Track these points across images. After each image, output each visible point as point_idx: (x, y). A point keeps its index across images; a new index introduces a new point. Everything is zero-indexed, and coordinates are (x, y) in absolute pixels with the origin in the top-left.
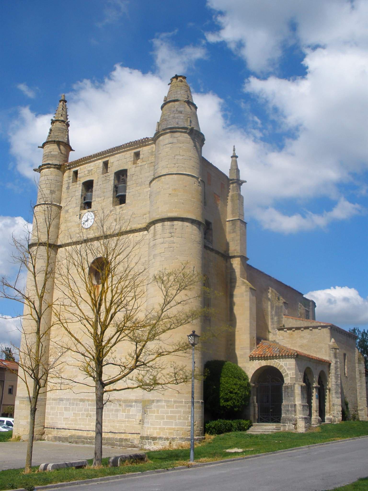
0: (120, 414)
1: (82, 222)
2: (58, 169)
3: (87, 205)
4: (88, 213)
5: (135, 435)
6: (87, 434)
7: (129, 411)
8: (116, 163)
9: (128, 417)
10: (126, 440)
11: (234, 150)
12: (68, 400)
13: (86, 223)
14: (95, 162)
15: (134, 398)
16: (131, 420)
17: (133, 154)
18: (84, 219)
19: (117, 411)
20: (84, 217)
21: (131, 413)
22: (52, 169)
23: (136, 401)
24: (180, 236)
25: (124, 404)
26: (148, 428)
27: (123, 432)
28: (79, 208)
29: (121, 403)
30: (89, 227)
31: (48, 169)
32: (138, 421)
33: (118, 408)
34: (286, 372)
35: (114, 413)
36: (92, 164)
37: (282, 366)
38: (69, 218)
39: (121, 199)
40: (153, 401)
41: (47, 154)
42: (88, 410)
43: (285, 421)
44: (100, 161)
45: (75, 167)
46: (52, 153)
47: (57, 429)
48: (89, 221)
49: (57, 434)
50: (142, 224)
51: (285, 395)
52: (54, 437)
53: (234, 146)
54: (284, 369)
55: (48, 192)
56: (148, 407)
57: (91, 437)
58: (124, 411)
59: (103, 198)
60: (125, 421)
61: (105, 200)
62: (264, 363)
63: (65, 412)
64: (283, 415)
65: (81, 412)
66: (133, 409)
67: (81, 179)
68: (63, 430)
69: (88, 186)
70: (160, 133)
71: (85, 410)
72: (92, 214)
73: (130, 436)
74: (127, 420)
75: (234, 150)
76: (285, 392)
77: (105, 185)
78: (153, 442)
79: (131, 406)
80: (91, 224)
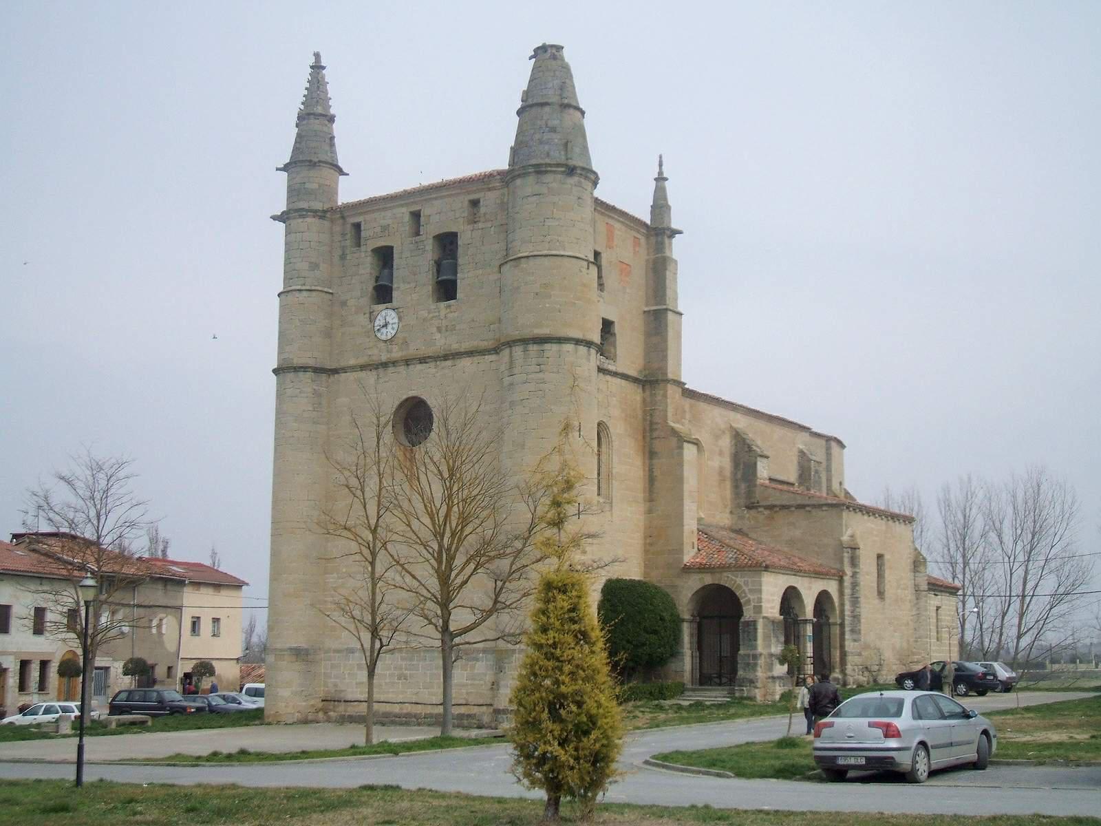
1: (376, 328)
2: (321, 218)
3: (383, 294)
5: (485, 708)
6: (401, 709)
7: (473, 667)
10: (469, 716)
11: (661, 165)
13: (384, 330)
14: (395, 211)
16: (477, 682)
17: (466, 203)
18: (379, 322)
20: (379, 317)
21: (476, 671)
22: (309, 220)
24: (555, 370)
27: (464, 702)
30: (389, 337)
31: (300, 220)
34: (746, 596)
36: (389, 214)
37: (739, 586)
39: (446, 290)
42: (401, 669)
43: (743, 682)
44: (404, 210)
45: (355, 215)
46: (307, 185)
48: (390, 327)
49: (345, 711)
50: (487, 340)
51: (744, 638)
53: (661, 157)
54: (744, 592)
55: (305, 266)
56: (506, 661)
57: (407, 714)
59: (413, 285)
60: (467, 685)
61: (417, 289)
62: (708, 579)
63: (359, 672)
64: (741, 673)
66: (479, 664)
67: (369, 242)
69: (385, 256)
70: (517, 173)
72: (393, 314)
73: (475, 710)
74: (469, 682)
75: (661, 165)
76: (744, 632)
79: (477, 660)
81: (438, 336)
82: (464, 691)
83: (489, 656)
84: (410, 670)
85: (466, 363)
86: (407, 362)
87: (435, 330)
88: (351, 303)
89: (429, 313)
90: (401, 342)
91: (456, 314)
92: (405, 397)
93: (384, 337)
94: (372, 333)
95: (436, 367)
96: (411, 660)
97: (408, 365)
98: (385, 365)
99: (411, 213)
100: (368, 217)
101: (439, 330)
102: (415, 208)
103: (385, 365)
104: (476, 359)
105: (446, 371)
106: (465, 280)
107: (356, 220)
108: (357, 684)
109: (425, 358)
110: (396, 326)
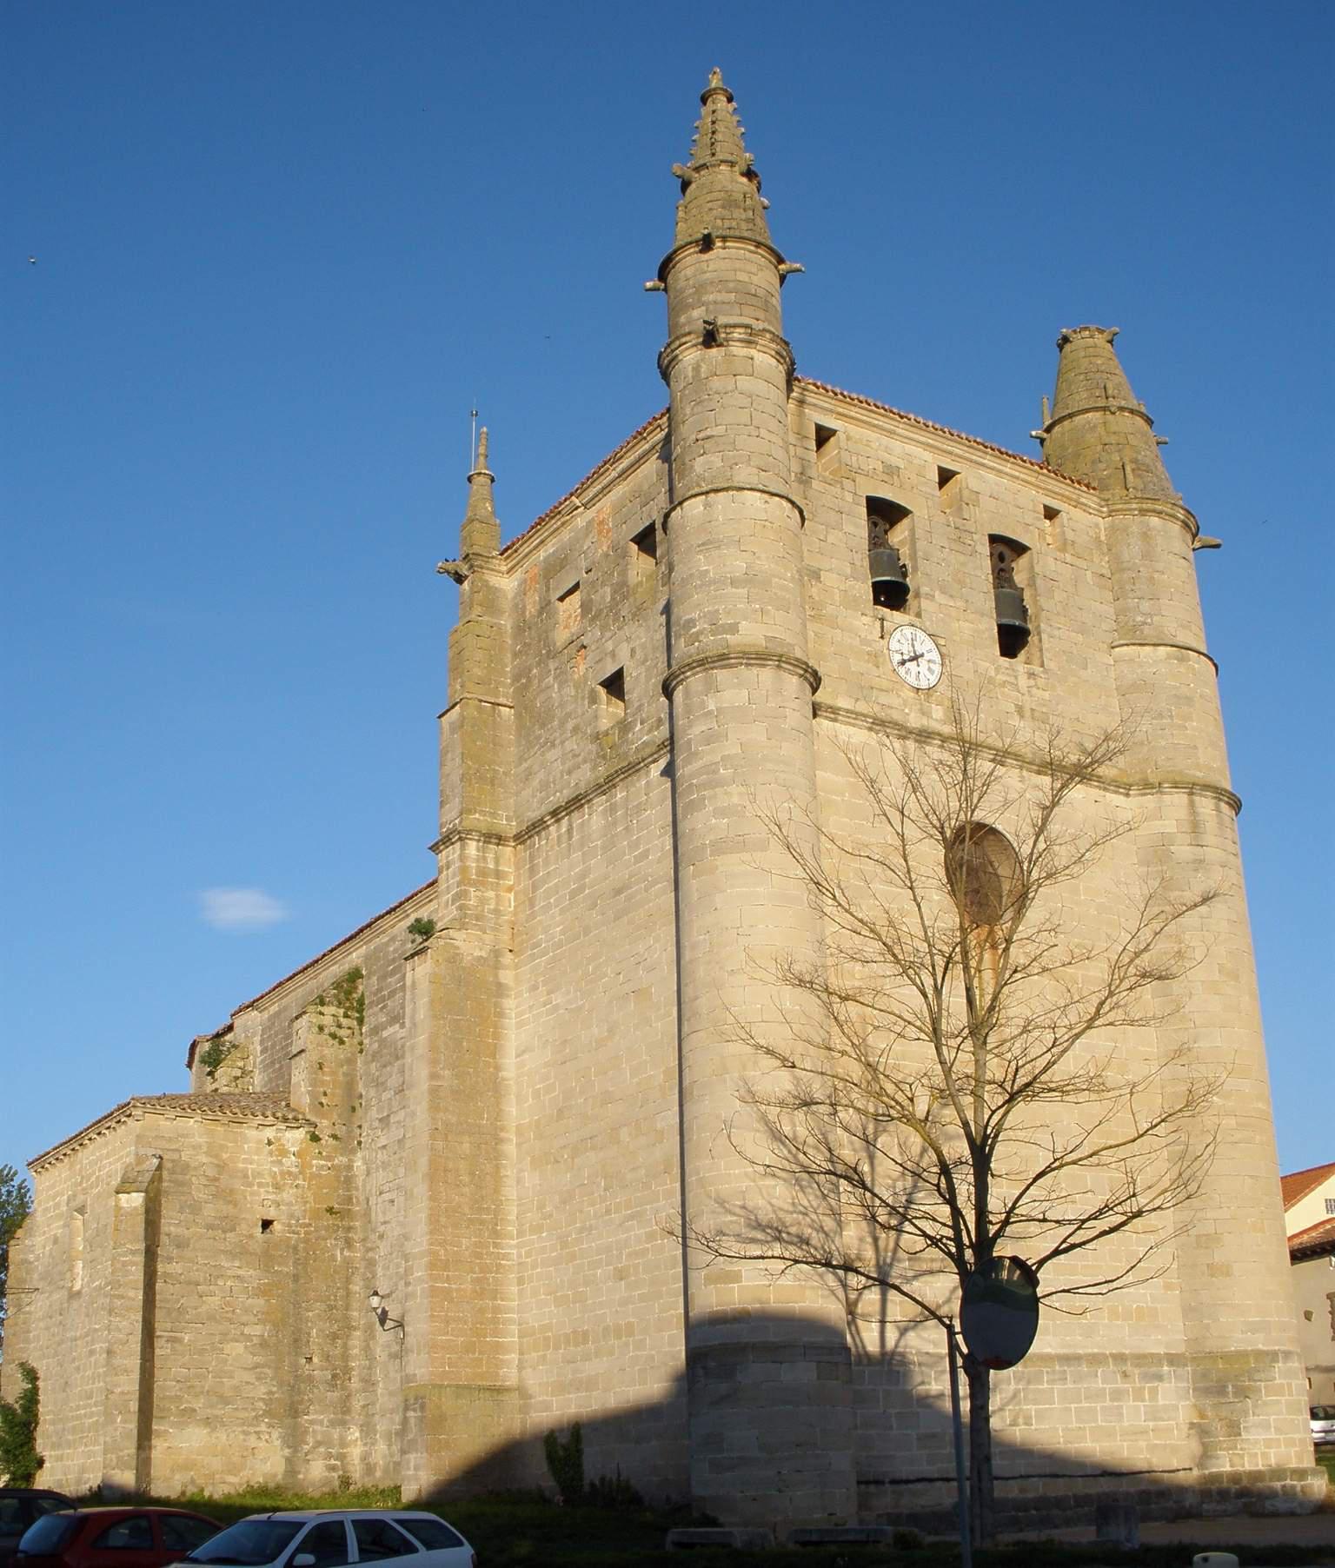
0: (1129, 1404)
4: (912, 629)
6: (1022, 1490)
7: (1154, 1392)
8: (985, 501)
9: (1153, 1415)
19: (1117, 1395)
21: (1161, 1402)
23: (1173, 1359)
25: (1137, 1371)
26: (1268, 1443)
29: (1129, 1368)
30: (924, 684)
32: (1185, 1428)
33: (1120, 1384)
35: (1108, 1403)
36: (896, 445)
38: (830, 609)
40: (1273, 1356)
41: (761, 292)
44: (928, 456)
47: (894, 1482)
52: (888, 1514)
58: (1138, 1396)
60: (1144, 1432)
68: (919, 1486)
74: (1151, 1424)
77: (962, 558)
79: (1160, 1378)
80: (933, 680)
82: (1143, 1444)
87: (1012, 708)
89: (997, 670)
91: (1046, 695)
93: (912, 680)
100: (854, 430)
107: (829, 422)
108: (919, 1439)
110: (937, 668)
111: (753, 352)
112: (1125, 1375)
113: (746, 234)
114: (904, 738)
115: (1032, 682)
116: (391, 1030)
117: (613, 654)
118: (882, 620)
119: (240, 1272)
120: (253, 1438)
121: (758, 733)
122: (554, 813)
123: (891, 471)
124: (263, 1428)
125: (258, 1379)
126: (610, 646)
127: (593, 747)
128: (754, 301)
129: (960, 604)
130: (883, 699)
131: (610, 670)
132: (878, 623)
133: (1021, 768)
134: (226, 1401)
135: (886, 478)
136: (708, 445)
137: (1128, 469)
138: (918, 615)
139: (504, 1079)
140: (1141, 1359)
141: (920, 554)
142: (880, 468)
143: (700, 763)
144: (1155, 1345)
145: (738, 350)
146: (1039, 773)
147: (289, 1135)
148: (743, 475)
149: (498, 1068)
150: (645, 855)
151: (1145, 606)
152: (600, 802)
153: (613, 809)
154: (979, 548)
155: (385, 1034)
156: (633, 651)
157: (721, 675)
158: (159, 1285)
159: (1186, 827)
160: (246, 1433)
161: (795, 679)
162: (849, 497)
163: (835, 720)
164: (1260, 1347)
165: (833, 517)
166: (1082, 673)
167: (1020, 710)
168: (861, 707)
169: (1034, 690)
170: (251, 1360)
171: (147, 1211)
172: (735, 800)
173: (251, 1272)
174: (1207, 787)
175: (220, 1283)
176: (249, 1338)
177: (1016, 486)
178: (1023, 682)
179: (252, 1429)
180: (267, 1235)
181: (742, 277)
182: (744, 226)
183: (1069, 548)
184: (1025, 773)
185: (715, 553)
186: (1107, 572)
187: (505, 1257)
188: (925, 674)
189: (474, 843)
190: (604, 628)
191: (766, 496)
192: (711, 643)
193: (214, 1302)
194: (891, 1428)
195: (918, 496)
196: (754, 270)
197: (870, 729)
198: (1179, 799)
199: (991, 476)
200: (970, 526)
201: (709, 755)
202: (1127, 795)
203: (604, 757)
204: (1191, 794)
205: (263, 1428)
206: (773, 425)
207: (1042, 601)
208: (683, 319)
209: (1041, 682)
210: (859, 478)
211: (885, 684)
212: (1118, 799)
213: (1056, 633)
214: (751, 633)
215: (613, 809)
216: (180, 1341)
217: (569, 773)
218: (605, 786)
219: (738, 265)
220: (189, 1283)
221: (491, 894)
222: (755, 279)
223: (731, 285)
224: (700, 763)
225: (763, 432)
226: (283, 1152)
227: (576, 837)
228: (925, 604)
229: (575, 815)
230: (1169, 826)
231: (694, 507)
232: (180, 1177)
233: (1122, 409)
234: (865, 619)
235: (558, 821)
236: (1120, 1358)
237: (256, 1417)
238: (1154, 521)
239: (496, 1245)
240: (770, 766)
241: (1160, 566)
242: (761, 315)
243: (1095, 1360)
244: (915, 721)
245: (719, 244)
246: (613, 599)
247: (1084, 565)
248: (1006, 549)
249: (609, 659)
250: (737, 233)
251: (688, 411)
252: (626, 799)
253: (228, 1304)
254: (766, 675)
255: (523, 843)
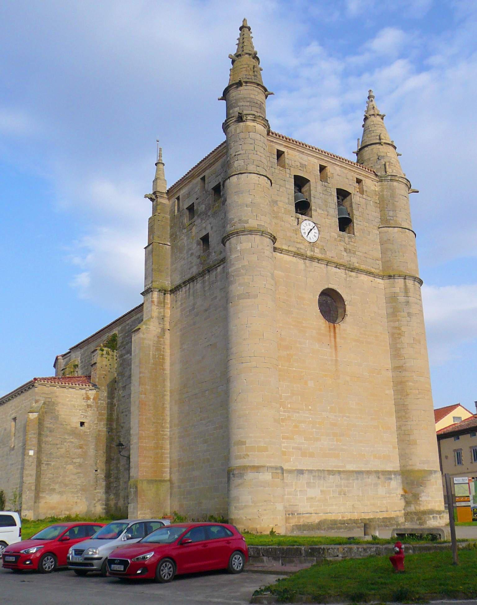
3: (303, 207)
7: (389, 485)
8: (336, 177)
12: (310, 471)
14: (310, 158)
15: (392, 470)
19: (376, 485)
23: (395, 473)
28: (293, 208)
30: (312, 241)
32: (400, 496)
36: (305, 157)
41: (259, 102)
44: (316, 161)
65: (332, 489)
70: (397, 179)
71: (336, 486)
77: (327, 197)
78: (438, 516)
79: (391, 479)
80: (315, 239)
81: (345, 254)
82: (385, 502)
83: (398, 477)
84: (347, 486)
85: (364, 278)
86: (328, 263)
87: (343, 249)
88: (280, 204)
90: (320, 247)
92: (326, 287)
94: (297, 231)
95: (346, 274)
96: (348, 479)
97: (327, 265)
98: (312, 259)
99: (320, 165)
100: (290, 151)
101: (345, 250)
102: (324, 164)
103: (312, 259)
104: (371, 278)
105: (352, 279)
106: (358, 223)
107: (282, 149)
108: (307, 499)
109: (341, 265)
110: (317, 235)
111: (255, 124)
112: (379, 478)
113: (253, 81)
114: (305, 259)
115: (350, 240)
116: (126, 356)
117: (205, 228)
118: (298, 219)
119: (72, 440)
120: (76, 498)
121: (254, 258)
122: (184, 283)
123: (303, 166)
124: (79, 495)
125: (78, 478)
126: (204, 225)
127: (198, 260)
128: (257, 105)
129: (326, 213)
130: (298, 246)
131: (204, 233)
132: (297, 220)
133: (345, 270)
134: (66, 485)
135: (301, 168)
136: (239, 157)
137: (387, 164)
138: (311, 217)
139: (166, 374)
140: (384, 472)
141: (312, 195)
142: (299, 165)
143: (234, 268)
144: (389, 467)
145: (250, 123)
146: (351, 271)
147: (90, 392)
148: (251, 168)
149: (164, 370)
150: (216, 298)
151: (391, 213)
152: (200, 280)
153: (204, 282)
154: (333, 193)
155: (124, 357)
156: (212, 228)
157: (243, 238)
158: (43, 445)
159: (403, 290)
160: (73, 497)
161: (268, 239)
162: (288, 176)
163: (281, 253)
164: (426, 469)
165: (282, 183)
166: (368, 237)
167: (345, 250)
168: (291, 249)
169: (351, 243)
170: (75, 471)
171: (39, 419)
172: (246, 281)
173: (76, 440)
174: (410, 276)
175: (65, 444)
176: (75, 463)
177: (346, 171)
178: (347, 239)
179: (75, 495)
180: (82, 428)
181: (252, 96)
182: (253, 77)
183: (365, 193)
184: (347, 271)
185: (241, 195)
186: (378, 202)
187: (165, 435)
188: (313, 237)
189: (156, 293)
190: (202, 220)
191: (259, 176)
192: (239, 226)
193: (63, 451)
194: (297, 495)
195: (313, 175)
196: (257, 94)
197: (293, 256)
198: (401, 281)
199: (338, 168)
200: (330, 185)
201: (238, 265)
202: (383, 279)
203: (202, 264)
204: (405, 279)
205: (79, 495)
206: (262, 150)
207: (355, 212)
208: (231, 111)
209: (353, 240)
210: (292, 169)
211: (299, 241)
212: (380, 281)
213: (359, 223)
214: (253, 223)
215: (204, 282)
216: (50, 464)
217: (190, 269)
218: (202, 274)
219: (251, 92)
220: (54, 444)
221: (162, 310)
222: (257, 98)
223: (248, 99)
224: (234, 268)
225: (258, 153)
226: (88, 398)
227: (191, 291)
228: (313, 213)
229: (191, 284)
230: (397, 290)
231: (234, 179)
232: (52, 407)
233: (385, 143)
234: (292, 218)
235: (186, 286)
236: (377, 472)
237: (77, 491)
238: (395, 184)
239: (163, 431)
240: (258, 269)
241: (397, 200)
242: (258, 110)
243: (369, 473)
244: (309, 253)
245: (244, 84)
246: (205, 209)
247: (369, 199)
248: (342, 194)
249: (203, 230)
250: (251, 80)
251: (232, 144)
252: (209, 278)
253: (68, 451)
254: (258, 238)
255: (173, 293)
